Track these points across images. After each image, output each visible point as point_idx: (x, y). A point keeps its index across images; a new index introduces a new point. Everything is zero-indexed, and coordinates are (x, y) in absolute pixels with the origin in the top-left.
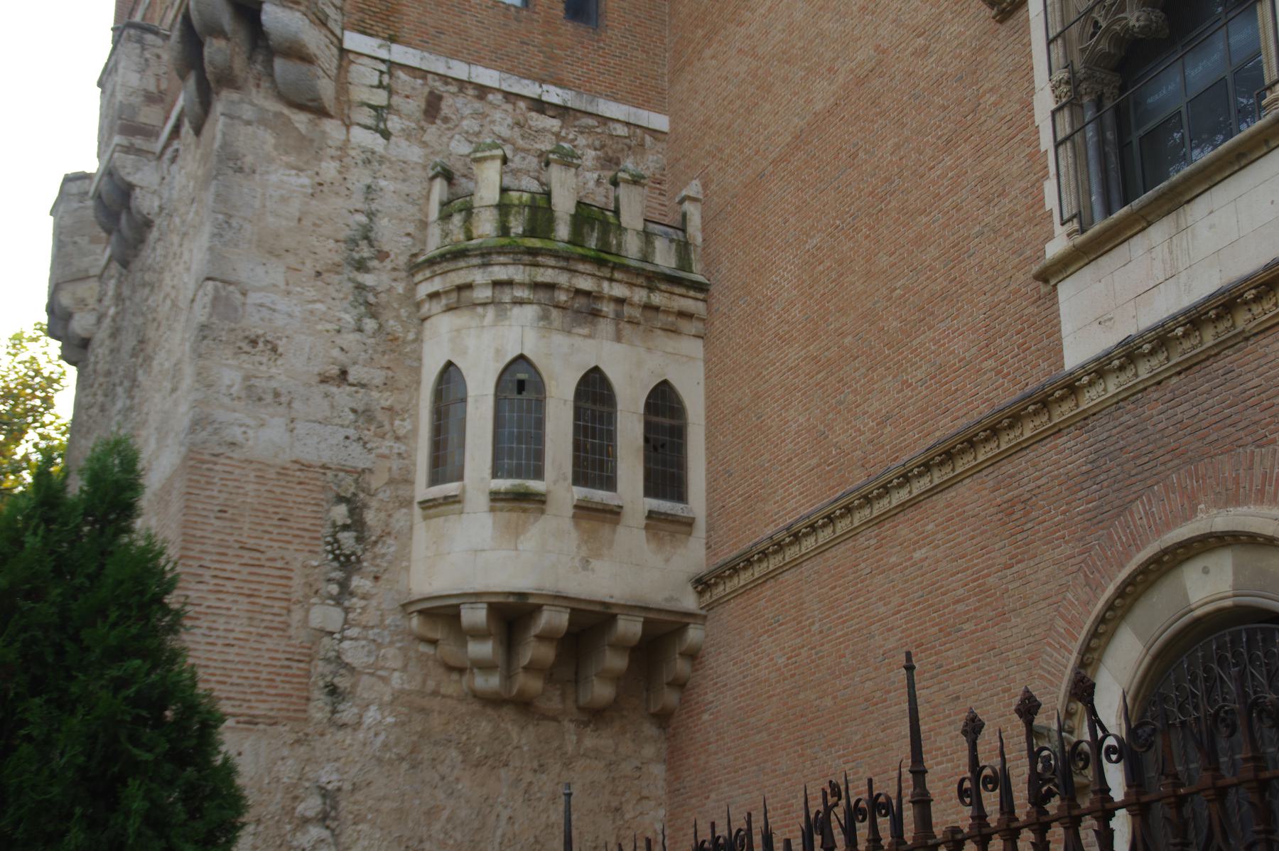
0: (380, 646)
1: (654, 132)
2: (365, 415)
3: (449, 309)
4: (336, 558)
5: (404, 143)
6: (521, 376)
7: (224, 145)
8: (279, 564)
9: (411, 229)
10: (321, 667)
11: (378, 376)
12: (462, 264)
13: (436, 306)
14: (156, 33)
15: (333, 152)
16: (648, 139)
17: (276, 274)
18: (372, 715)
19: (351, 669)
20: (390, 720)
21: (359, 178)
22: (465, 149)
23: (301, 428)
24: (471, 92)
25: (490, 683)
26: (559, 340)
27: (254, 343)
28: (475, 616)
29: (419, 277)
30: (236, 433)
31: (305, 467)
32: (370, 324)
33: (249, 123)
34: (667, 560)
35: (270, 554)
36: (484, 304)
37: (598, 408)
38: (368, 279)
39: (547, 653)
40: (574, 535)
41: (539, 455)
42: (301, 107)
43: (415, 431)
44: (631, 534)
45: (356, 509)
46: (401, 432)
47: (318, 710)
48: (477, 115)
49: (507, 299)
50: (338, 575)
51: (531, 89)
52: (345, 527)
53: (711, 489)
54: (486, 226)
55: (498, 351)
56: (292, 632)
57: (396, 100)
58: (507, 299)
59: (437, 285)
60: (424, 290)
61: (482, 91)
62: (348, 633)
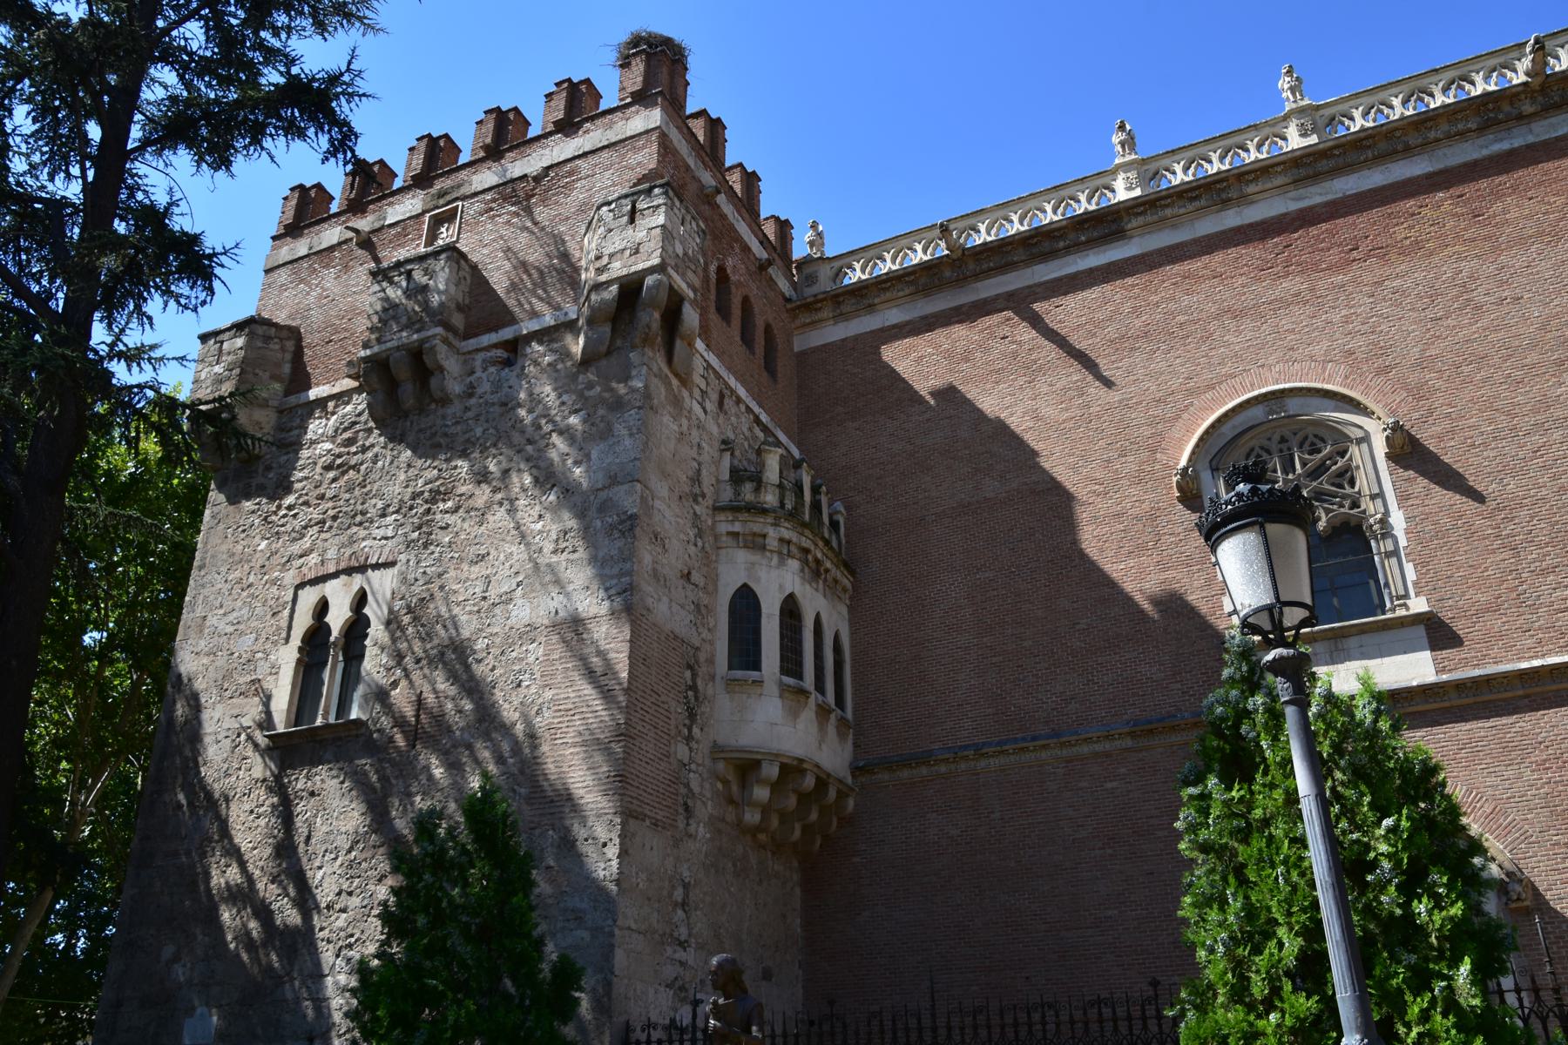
8: (666, 706)
28: (771, 771)
31: (676, 638)
41: (800, 664)
42: (677, 375)
45: (694, 676)
50: (687, 722)
54: (770, 498)
59: (737, 527)
60: (723, 528)
62: (693, 766)
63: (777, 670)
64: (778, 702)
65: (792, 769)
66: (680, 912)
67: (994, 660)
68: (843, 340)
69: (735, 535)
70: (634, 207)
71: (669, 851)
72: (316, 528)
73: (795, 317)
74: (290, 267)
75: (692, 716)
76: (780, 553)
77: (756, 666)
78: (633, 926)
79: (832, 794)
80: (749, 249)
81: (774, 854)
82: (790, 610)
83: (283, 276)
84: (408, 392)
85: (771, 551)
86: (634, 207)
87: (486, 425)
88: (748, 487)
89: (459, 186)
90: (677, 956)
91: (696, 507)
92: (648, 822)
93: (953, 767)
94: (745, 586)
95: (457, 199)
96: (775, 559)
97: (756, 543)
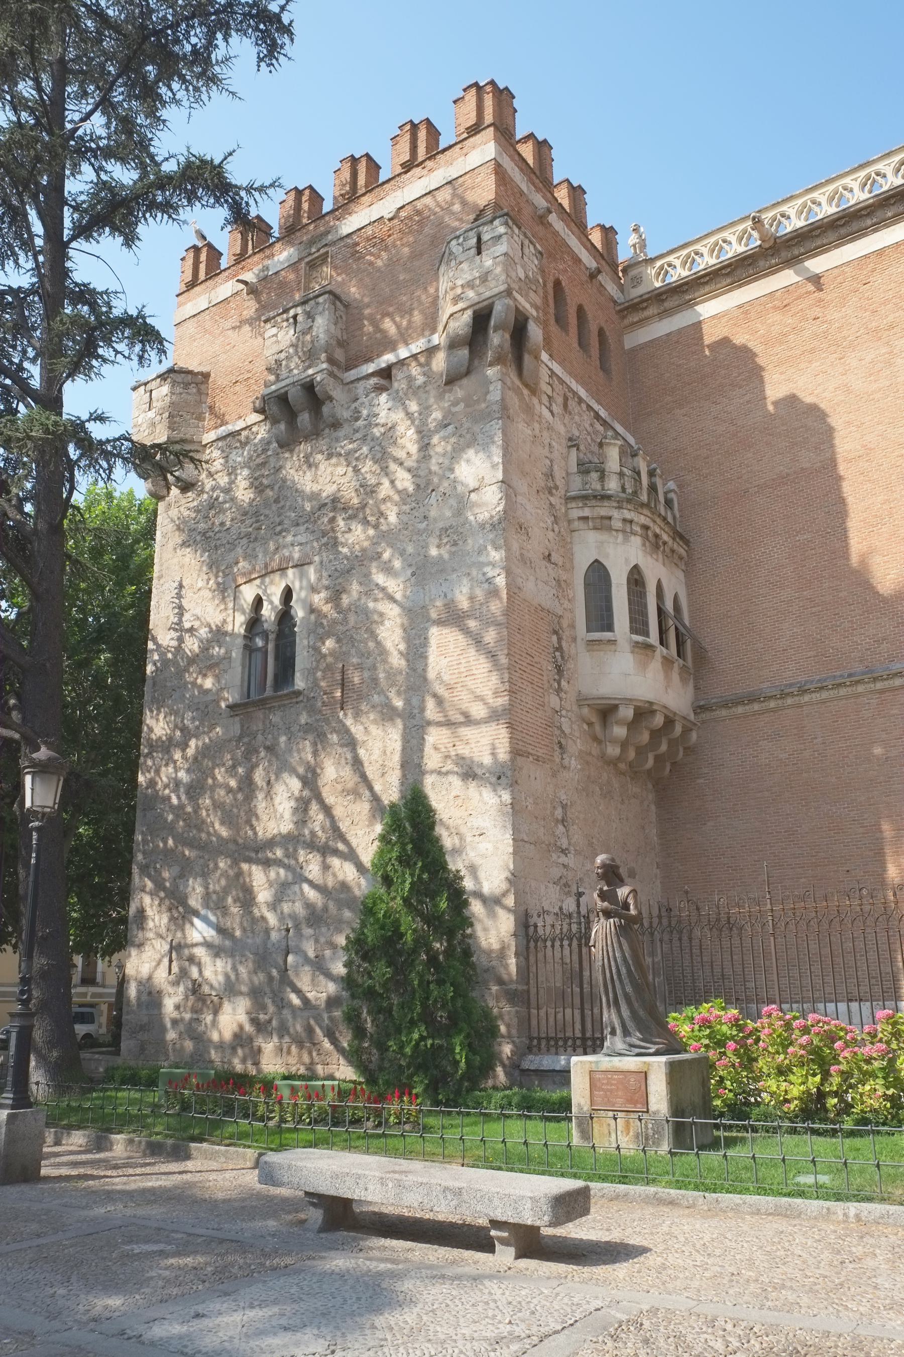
3: (595, 528)
6: (636, 576)
12: (606, 504)
14: (341, 301)
28: (627, 713)
29: (569, 506)
31: (543, 609)
36: (617, 531)
41: (646, 624)
42: (527, 386)
45: (560, 639)
50: (556, 677)
54: (613, 485)
59: (587, 512)
60: (575, 513)
62: (564, 712)
63: (627, 629)
64: (630, 657)
65: (643, 712)
66: (561, 827)
67: (814, 610)
68: (668, 335)
69: (585, 519)
70: (479, 239)
72: (245, 541)
73: (624, 317)
74: (195, 319)
75: (559, 670)
77: (610, 628)
78: (526, 839)
79: (678, 729)
80: (580, 260)
81: (632, 779)
82: (636, 579)
83: (190, 326)
84: (304, 418)
85: (617, 531)
86: (479, 239)
87: (372, 444)
88: (594, 475)
89: (328, 232)
90: (560, 860)
91: (551, 499)
92: (531, 758)
93: (780, 702)
94: (596, 561)
95: (326, 245)
97: (603, 524)
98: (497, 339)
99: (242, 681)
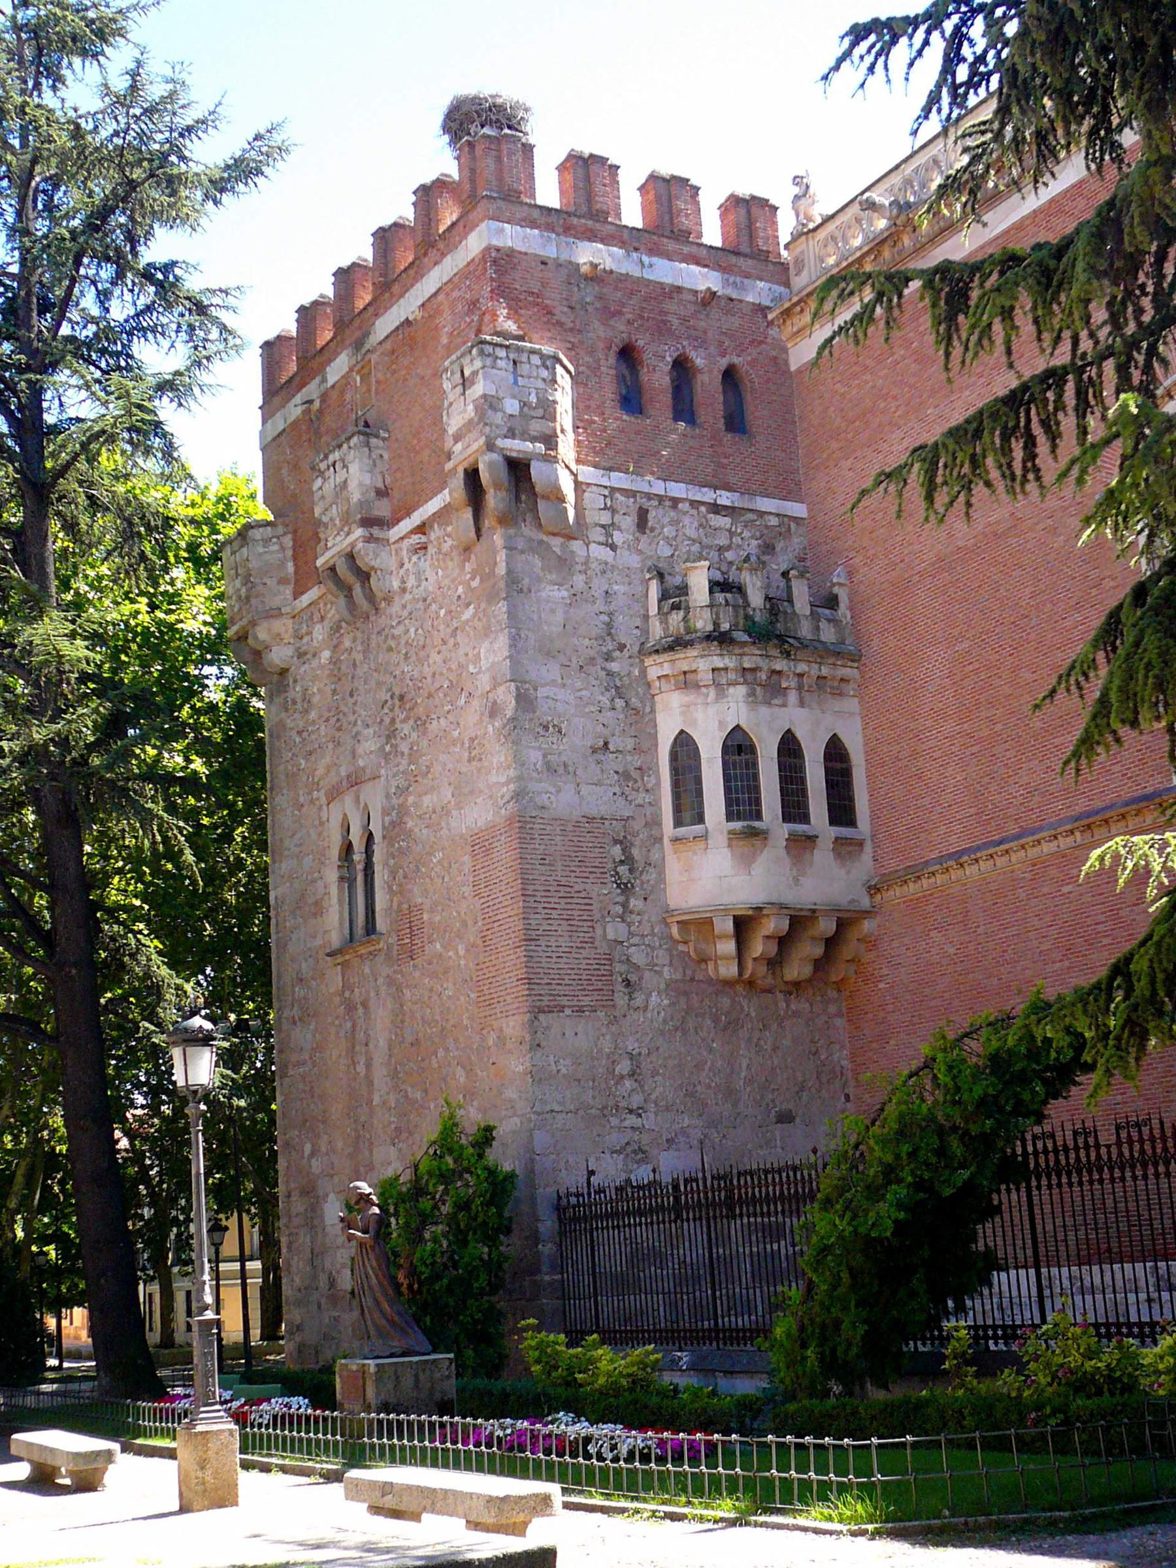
0: (653, 949)
1: (795, 519)
2: (626, 776)
4: (619, 886)
5: (626, 553)
7: (510, 572)
8: (582, 895)
9: (638, 623)
10: (619, 967)
11: (630, 743)
13: (665, 685)
15: (579, 567)
16: (793, 525)
17: (553, 671)
18: (654, 998)
19: (637, 967)
20: (666, 1002)
21: (599, 585)
22: (668, 552)
23: (585, 789)
24: (668, 503)
25: (729, 970)
26: (764, 710)
27: (546, 728)
30: (543, 799)
31: (591, 819)
32: (619, 703)
33: (523, 552)
34: (848, 872)
35: (577, 888)
37: (792, 760)
38: (614, 666)
39: (773, 949)
40: (787, 861)
43: (658, 784)
44: (823, 855)
46: (649, 786)
47: (621, 1000)
48: (674, 522)
49: (724, 681)
50: (620, 899)
51: (708, 495)
52: (622, 862)
53: (874, 816)
55: (720, 722)
56: (597, 944)
57: (617, 518)
58: (724, 681)
61: (675, 501)
64: (726, 852)
71: (604, 1030)
75: (625, 888)
76: (717, 685)
77: (700, 819)
78: (557, 1108)
90: (627, 1123)
92: (568, 1011)
96: (712, 693)
97: (686, 681)
98: (494, 500)
99: (341, 924)
